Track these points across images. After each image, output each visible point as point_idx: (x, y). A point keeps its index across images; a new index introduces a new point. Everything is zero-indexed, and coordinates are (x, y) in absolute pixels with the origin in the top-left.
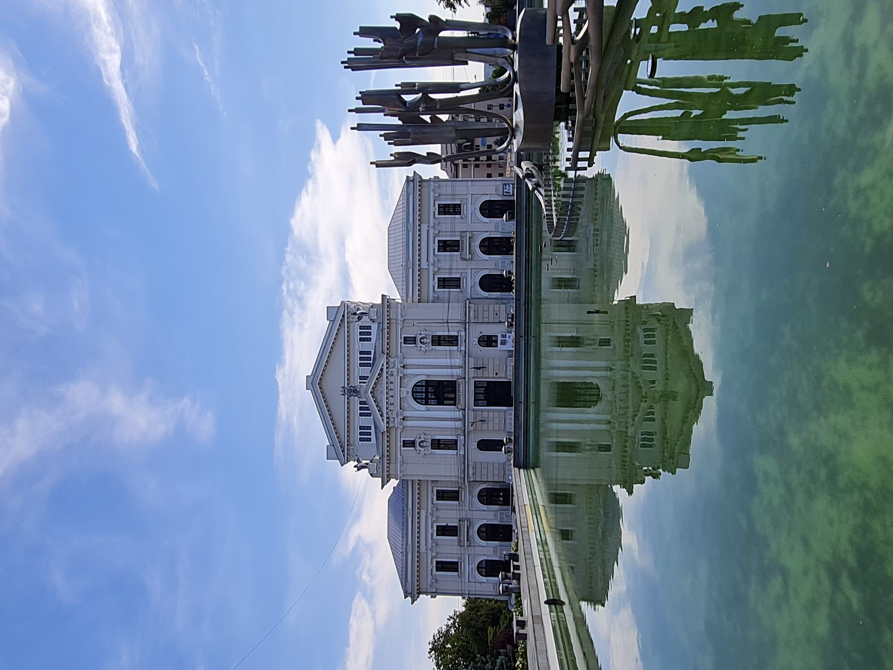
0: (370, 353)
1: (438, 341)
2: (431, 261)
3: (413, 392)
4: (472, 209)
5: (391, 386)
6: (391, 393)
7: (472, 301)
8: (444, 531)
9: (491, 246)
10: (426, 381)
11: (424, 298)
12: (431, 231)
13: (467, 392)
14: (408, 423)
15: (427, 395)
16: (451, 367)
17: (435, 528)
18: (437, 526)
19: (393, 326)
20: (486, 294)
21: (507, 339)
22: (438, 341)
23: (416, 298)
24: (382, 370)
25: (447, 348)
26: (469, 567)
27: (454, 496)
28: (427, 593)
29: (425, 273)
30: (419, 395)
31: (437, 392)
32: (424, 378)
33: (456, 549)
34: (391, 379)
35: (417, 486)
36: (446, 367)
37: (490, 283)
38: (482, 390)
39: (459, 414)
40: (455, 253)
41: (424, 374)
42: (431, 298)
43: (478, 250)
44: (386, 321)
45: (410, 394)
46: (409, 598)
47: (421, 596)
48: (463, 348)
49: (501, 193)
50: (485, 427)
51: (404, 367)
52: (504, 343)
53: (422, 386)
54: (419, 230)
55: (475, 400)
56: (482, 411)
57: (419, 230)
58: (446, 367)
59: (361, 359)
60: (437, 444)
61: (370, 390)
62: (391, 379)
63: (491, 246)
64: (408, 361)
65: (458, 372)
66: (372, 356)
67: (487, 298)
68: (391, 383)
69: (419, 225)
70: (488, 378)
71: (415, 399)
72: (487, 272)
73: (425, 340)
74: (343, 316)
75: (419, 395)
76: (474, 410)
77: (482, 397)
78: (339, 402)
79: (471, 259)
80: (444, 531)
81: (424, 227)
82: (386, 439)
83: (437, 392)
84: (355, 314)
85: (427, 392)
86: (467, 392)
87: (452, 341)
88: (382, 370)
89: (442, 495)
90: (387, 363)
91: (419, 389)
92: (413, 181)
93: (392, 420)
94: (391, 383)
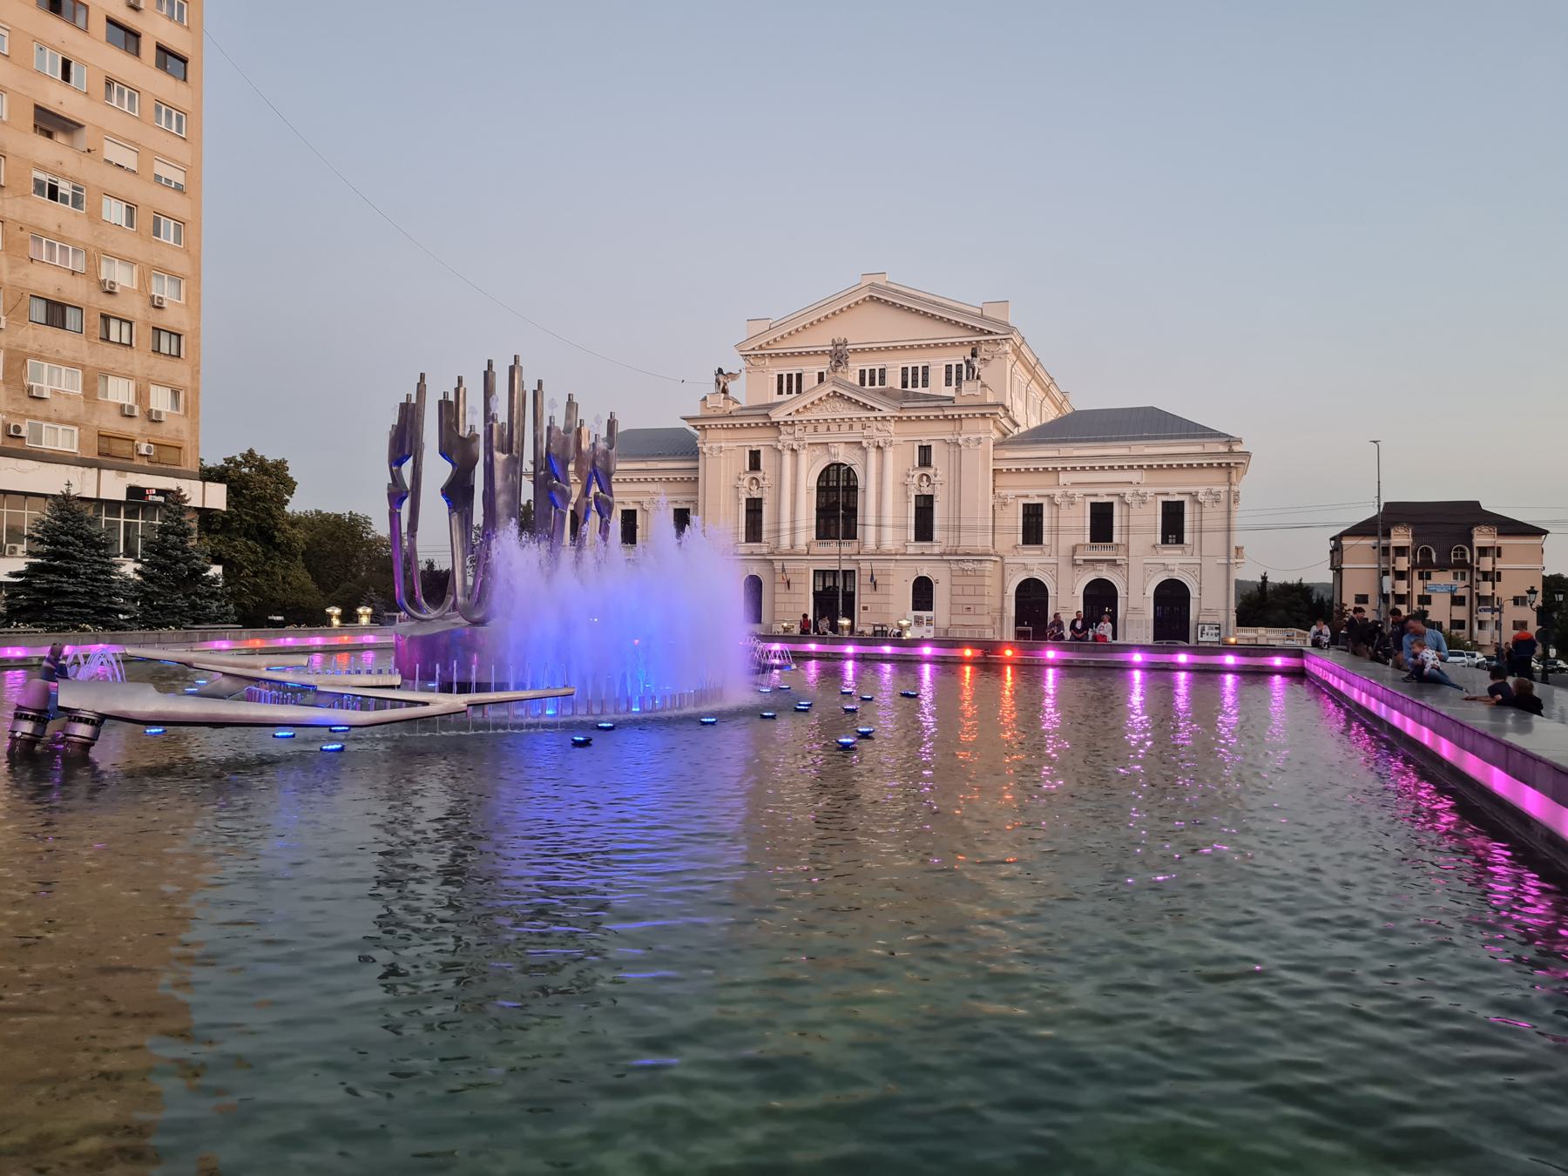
0: (925, 384)
1: (924, 508)
3: (839, 465)
4: (1175, 564)
5: (845, 427)
6: (834, 427)
7: (999, 566)
10: (856, 488)
11: (1001, 480)
12: (1128, 491)
13: (833, 555)
14: (787, 457)
17: (631, 507)
19: (949, 426)
20: (1011, 590)
21: (925, 627)
22: (924, 508)
23: (1004, 466)
24: (873, 409)
25: (912, 521)
31: (838, 505)
34: (857, 426)
35: (686, 476)
37: (1032, 597)
42: (1004, 492)
44: (956, 412)
45: (834, 460)
48: (911, 550)
49: (1202, 619)
50: (781, 588)
51: (878, 447)
52: (918, 621)
53: (848, 480)
54: (1131, 467)
55: (824, 572)
59: (915, 369)
60: (754, 508)
62: (857, 426)
63: (1101, 598)
64: (890, 454)
65: (871, 543)
66: (920, 389)
67: (1003, 592)
68: (851, 427)
69: (1140, 467)
71: (827, 469)
72: (1051, 593)
74: (990, 333)
75: (833, 475)
77: (829, 583)
78: (822, 339)
79: (1074, 565)
81: (1134, 476)
82: (753, 421)
83: (838, 505)
84: (974, 355)
86: (833, 555)
87: (924, 530)
88: (873, 409)
92: (1231, 452)
93: (789, 430)
94: (851, 427)
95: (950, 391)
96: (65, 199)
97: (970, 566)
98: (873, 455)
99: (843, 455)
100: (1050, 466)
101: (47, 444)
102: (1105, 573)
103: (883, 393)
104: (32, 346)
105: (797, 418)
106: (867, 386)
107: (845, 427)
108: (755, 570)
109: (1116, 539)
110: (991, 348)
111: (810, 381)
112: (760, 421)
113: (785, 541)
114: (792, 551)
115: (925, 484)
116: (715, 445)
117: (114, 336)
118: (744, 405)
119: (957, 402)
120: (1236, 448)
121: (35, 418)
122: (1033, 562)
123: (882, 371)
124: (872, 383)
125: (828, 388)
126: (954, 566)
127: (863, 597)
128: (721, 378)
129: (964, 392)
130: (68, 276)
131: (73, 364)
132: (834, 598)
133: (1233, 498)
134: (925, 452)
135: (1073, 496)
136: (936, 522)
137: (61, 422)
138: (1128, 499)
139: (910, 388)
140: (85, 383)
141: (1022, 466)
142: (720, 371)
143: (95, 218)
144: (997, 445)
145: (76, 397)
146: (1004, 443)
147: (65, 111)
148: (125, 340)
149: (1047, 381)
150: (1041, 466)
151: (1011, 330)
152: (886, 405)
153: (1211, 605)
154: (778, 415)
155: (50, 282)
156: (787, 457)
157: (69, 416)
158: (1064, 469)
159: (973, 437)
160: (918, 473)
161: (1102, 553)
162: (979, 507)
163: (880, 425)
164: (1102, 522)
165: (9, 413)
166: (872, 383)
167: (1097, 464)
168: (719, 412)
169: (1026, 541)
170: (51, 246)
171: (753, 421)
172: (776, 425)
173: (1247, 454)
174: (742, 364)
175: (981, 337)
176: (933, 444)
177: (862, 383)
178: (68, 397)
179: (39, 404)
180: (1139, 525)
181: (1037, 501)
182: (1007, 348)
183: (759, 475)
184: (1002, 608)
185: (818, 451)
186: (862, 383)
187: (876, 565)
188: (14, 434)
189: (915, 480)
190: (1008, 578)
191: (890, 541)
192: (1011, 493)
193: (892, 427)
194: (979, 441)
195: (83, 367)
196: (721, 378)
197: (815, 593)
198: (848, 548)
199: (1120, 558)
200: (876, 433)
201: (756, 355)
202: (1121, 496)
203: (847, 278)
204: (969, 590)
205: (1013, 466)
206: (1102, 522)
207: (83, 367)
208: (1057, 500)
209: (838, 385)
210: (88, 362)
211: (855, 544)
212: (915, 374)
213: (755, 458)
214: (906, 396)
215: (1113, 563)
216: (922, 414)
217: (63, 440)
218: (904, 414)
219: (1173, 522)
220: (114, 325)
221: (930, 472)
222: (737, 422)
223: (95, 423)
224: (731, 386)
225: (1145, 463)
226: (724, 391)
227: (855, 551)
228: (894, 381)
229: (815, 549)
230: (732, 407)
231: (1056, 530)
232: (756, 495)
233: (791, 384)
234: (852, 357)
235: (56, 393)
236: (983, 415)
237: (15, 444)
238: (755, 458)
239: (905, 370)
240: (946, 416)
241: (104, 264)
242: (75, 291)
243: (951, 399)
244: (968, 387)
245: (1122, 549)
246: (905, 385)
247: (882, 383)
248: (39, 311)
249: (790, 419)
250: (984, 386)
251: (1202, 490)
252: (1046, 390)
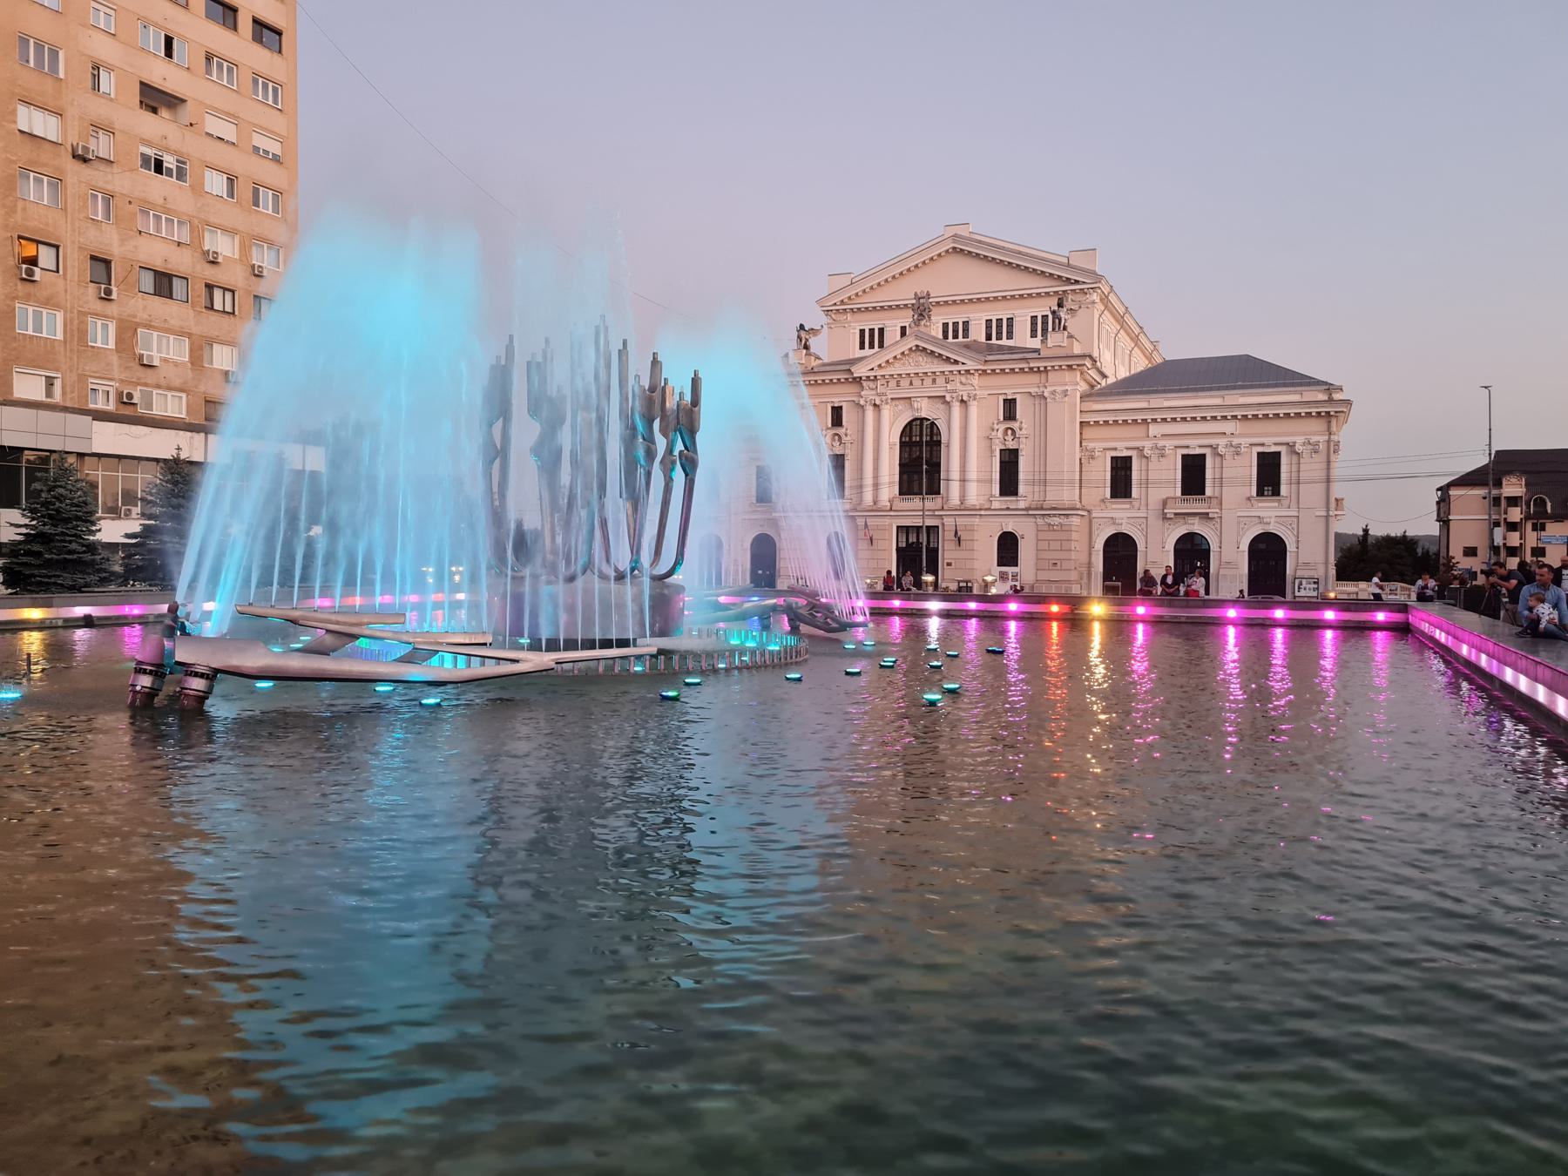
0: (1010, 336)
1: (1009, 462)
3: (922, 420)
4: (1270, 516)
5: (928, 381)
6: (917, 382)
7: (1086, 520)
9: (1268, 557)
10: (939, 442)
11: (1088, 433)
12: (1222, 442)
13: (915, 511)
14: (870, 413)
16: (876, 486)
19: (1034, 378)
22: (1009, 462)
23: (1091, 418)
24: (956, 362)
25: (996, 476)
29: (1138, 431)
31: (921, 460)
32: (944, 439)
34: (940, 381)
36: (876, 477)
37: (1120, 552)
40: (1108, 490)
42: (1091, 445)
43: (1182, 530)
44: (1041, 364)
45: (917, 415)
48: (996, 505)
49: (1299, 574)
50: (864, 545)
51: (962, 401)
52: (1003, 577)
54: (1224, 418)
55: (908, 527)
57: (1224, 418)
58: (876, 477)
59: (999, 321)
61: (922, 344)
62: (940, 381)
63: (1192, 553)
64: (974, 409)
66: (1004, 342)
67: (1091, 547)
68: (934, 381)
69: (1234, 417)
71: (910, 424)
72: (1140, 547)
74: (1077, 282)
75: (916, 430)
77: (912, 539)
78: (904, 292)
79: (1165, 518)
81: (1228, 427)
82: (835, 377)
83: (921, 460)
84: (1060, 305)
86: (915, 511)
87: (1009, 484)
88: (956, 362)
90: (968, 371)
92: (1331, 400)
93: (872, 385)
94: (934, 381)
95: (1035, 343)
96: (169, 173)
97: (1056, 520)
98: (956, 409)
99: (926, 410)
100: (1139, 417)
101: (157, 411)
102: (1197, 527)
103: (967, 346)
104: (142, 316)
105: (880, 373)
106: (950, 339)
107: (928, 381)
109: (1208, 491)
110: (1078, 297)
111: (892, 335)
112: (842, 376)
113: (868, 497)
114: (875, 507)
115: (1009, 437)
116: (1059, 389)
117: (218, 305)
118: (826, 361)
119: (1043, 354)
120: (1336, 396)
121: (146, 385)
122: (1122, 517)
123: (966, 324)
124: (956, 336)
125: (911, 342)
126: (1040, 521)
127: (947, 552)
128: (803, 334)
129: (1050, 343)
130: (174, 247)
131: (181, 333)
132: (917, 556)
133: (1333, 448)
134: (1010, 407)
135: (1163, 448)
136: (1021, 476)
137: (170, 389)
138: (1221, 450)
139: (994, 341)
140: (191, 350)
141: (1111, 419)
142: (802, 327)
143: (198, 189)
144: (1084, 397)
145: (183, 363)
146: (1092, 394)
147: (168, 87)
148: (228, 309)
149: (1137, 331)
150: (1130, 418)
151: (1099, 278)
152: (971, 358)
153: (1309, 558)
154: (860, 371)
155: (157, 253)
156: (870, 413)
157: (177, 382)
158: (1154, 420)
159: (1059, 389)
160: (1002, 427)
161: (1195, 506)
162: (1066, 462)
163: (963, 379)
164: (1193, 474)
165: (122, 381)
166: (956, 336)
167: (1189, 415)
168: (1062, 352)
169: (1114, 495)
170: (158, 218)
171: (835, 377)
172: (858, 381)
173: (1348, 402)
174: (824, 319)
175: (1067, 287)
176: (1018, 397)
177: (946, 337)
178: (176, 364)
179: (149, 371)
180: (1233, 477)
181: (1125, 453)
182: (1095, 297)
183: (841, 431)
184: (1090, 565)
185: (901, 406)
186: (946, 337)
187: (960, 521)
188: (126, 400)
189: (1000, 434)
191: (974, 496)
192: (1098, 446)
193: (975, 380)
194: (1065, 393)
195: (190, 335)
196: (803, 334)
197: (898, 549)
198: (932, 503)
199: (1213, 511)
200: (959, 387)
201: (838, 310)
202: (1214, 448)
203: (928, 230)
204: (1056, 545)
205: (1101, 418)
206: (1193, 474)
207: (190, 335)
208: (1147, 452)
209: (921, 339)
210: (195, 330)
211: (939, 500)
212: (999, 326)
213: (837, 412)
214: (990, 349)
215: (1205, 516)
216: (1007, 366)
217: (171, 405)
218: (988, 367)
219: (1269, 474)
220: (218, 294)
221: (1015, 425)
222: (819, 378)
223: (202, 388)
224: (813, 342)
225: (1239, 413)
226: (806, 347)
227: (939, 506)
228: (978, 334)
229: (899, 504)
230: (814, 363)
231: (1146, 483)
232: (1011, 445)
233: (873, 339)
234: (934, 311)
235: (165, 360)
236: (1070, 367)
237: (127, 411)
238: (837, 412)
239: (989, 322)
240: (1031, 369)
241: (207, 235)
242: (180, 262)
243: (1037, 351)
244: (1054, 339)
245: (1214, 502)
246: (989, 337)
247: (966, 335)
248: (148, 282)
249: (872, 374)
250: (1070, 336)
251: (1299, 440)
252: (1136, 340)
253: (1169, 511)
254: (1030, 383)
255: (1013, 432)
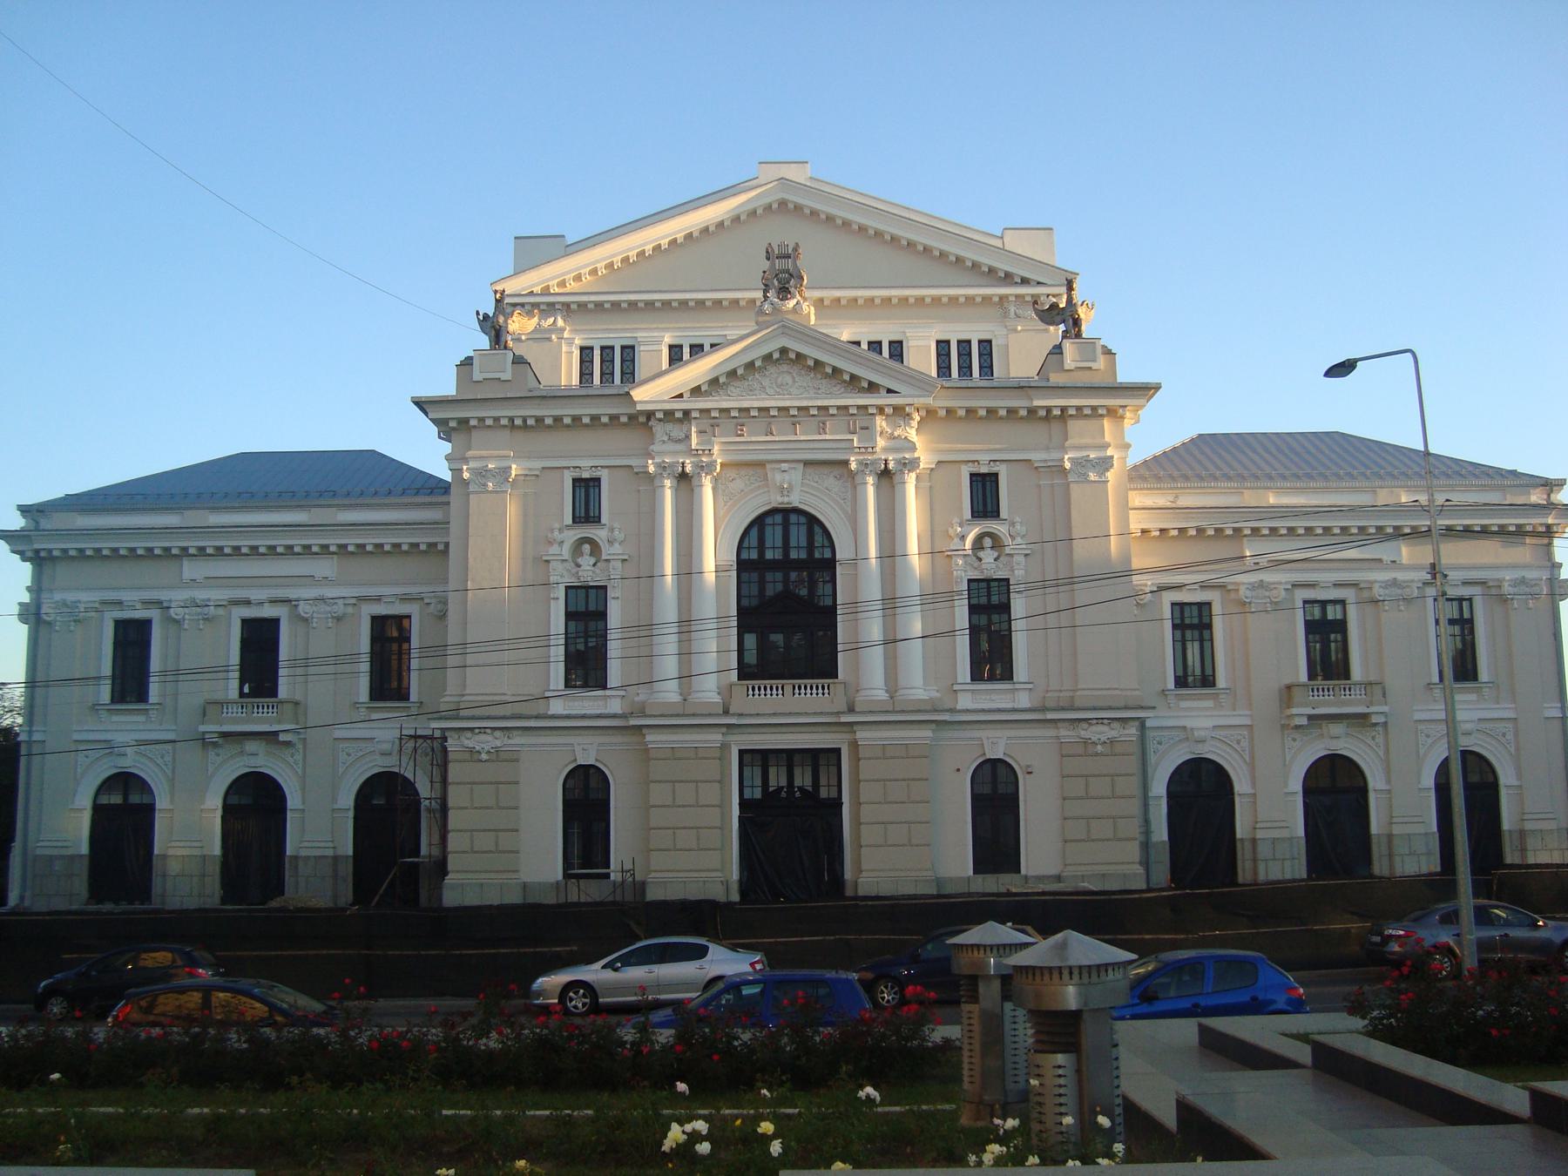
2: (1267, 577)
3: (786, 513)
8: (260, 642)
10: (830, 565)
13: (790, 714)
15: (774, 565)
17: (268, 612)
18: (275, 622)
19: (1036, 432)
20: (1159, 788)
24: (873, 387)
26: (131, 738)
27: (388, 681)
28: (36, 588)
30: (774, 536)
33: (194, 693)
38: (803, 779)
39: (708, 690)
41: (860, 545)
45: (777, 500)
46: (17, 522)
47: (26, 569)
53: (811, 547)
56: (723, 782)
61: (796, 346)
65: (874, 684)
70: (857, 804)
71: (759, 522)
73: (988, 556)
75: (774, 536)
76: (725, 747)
77: (777, 778)
80: (260, 642)
85: (785, 564)
86: (790, 714)
88: (873, 387)
89: (389, 638)
91: (798, 536)
93: (677, 431)
99: (800, 492)
108: (587, 752)
126: (1065, 733)
164: (1327, 640)
172: (644, 420)
184: (1147, 822)
190: (1152, 759)
191: (917, 685)
197: (743, 804)
206: (1327, 640)
213: (587, 489)
240: (1032, 411)
253: (1300, 712)
254: (1029, 444)
255: (997, 544)
